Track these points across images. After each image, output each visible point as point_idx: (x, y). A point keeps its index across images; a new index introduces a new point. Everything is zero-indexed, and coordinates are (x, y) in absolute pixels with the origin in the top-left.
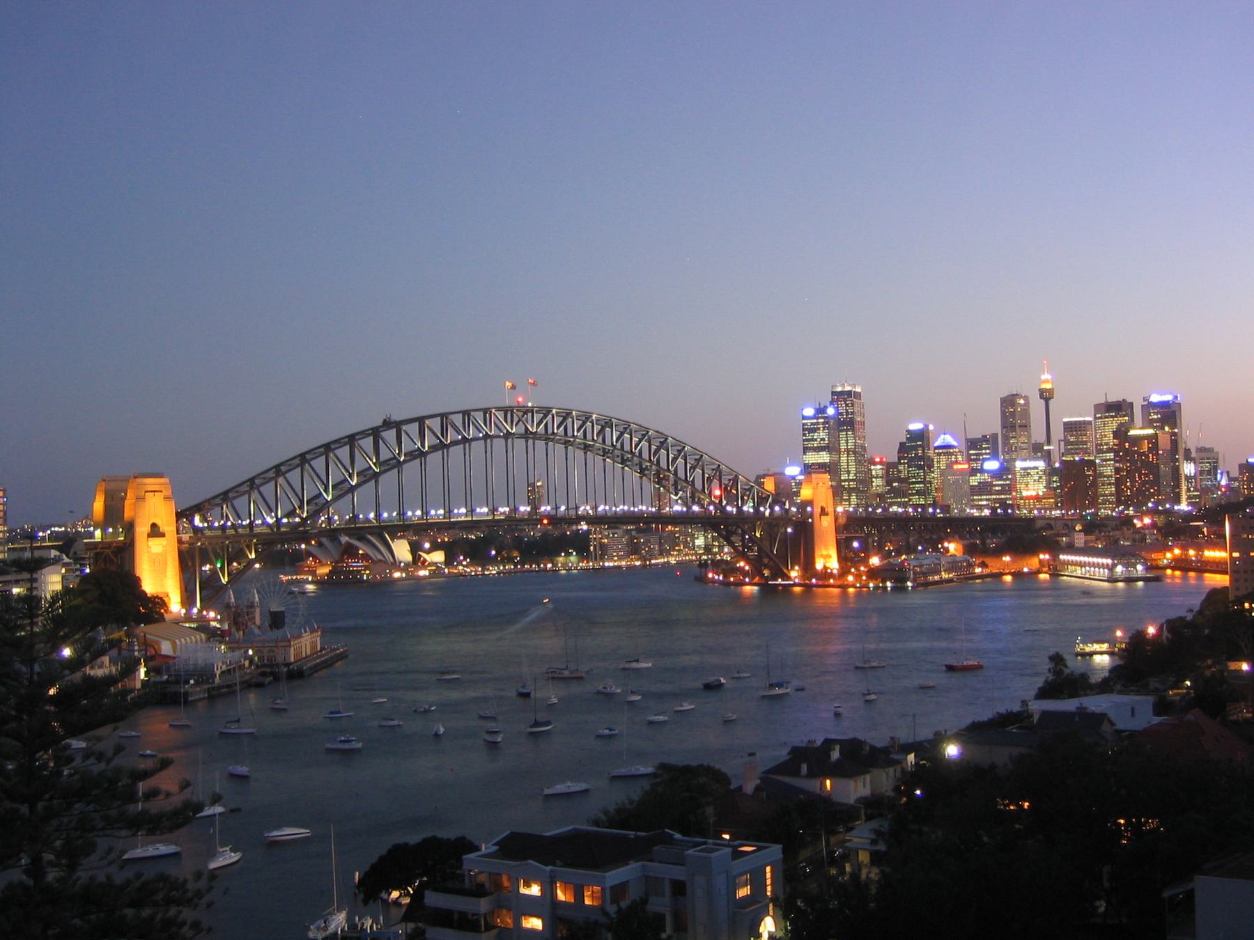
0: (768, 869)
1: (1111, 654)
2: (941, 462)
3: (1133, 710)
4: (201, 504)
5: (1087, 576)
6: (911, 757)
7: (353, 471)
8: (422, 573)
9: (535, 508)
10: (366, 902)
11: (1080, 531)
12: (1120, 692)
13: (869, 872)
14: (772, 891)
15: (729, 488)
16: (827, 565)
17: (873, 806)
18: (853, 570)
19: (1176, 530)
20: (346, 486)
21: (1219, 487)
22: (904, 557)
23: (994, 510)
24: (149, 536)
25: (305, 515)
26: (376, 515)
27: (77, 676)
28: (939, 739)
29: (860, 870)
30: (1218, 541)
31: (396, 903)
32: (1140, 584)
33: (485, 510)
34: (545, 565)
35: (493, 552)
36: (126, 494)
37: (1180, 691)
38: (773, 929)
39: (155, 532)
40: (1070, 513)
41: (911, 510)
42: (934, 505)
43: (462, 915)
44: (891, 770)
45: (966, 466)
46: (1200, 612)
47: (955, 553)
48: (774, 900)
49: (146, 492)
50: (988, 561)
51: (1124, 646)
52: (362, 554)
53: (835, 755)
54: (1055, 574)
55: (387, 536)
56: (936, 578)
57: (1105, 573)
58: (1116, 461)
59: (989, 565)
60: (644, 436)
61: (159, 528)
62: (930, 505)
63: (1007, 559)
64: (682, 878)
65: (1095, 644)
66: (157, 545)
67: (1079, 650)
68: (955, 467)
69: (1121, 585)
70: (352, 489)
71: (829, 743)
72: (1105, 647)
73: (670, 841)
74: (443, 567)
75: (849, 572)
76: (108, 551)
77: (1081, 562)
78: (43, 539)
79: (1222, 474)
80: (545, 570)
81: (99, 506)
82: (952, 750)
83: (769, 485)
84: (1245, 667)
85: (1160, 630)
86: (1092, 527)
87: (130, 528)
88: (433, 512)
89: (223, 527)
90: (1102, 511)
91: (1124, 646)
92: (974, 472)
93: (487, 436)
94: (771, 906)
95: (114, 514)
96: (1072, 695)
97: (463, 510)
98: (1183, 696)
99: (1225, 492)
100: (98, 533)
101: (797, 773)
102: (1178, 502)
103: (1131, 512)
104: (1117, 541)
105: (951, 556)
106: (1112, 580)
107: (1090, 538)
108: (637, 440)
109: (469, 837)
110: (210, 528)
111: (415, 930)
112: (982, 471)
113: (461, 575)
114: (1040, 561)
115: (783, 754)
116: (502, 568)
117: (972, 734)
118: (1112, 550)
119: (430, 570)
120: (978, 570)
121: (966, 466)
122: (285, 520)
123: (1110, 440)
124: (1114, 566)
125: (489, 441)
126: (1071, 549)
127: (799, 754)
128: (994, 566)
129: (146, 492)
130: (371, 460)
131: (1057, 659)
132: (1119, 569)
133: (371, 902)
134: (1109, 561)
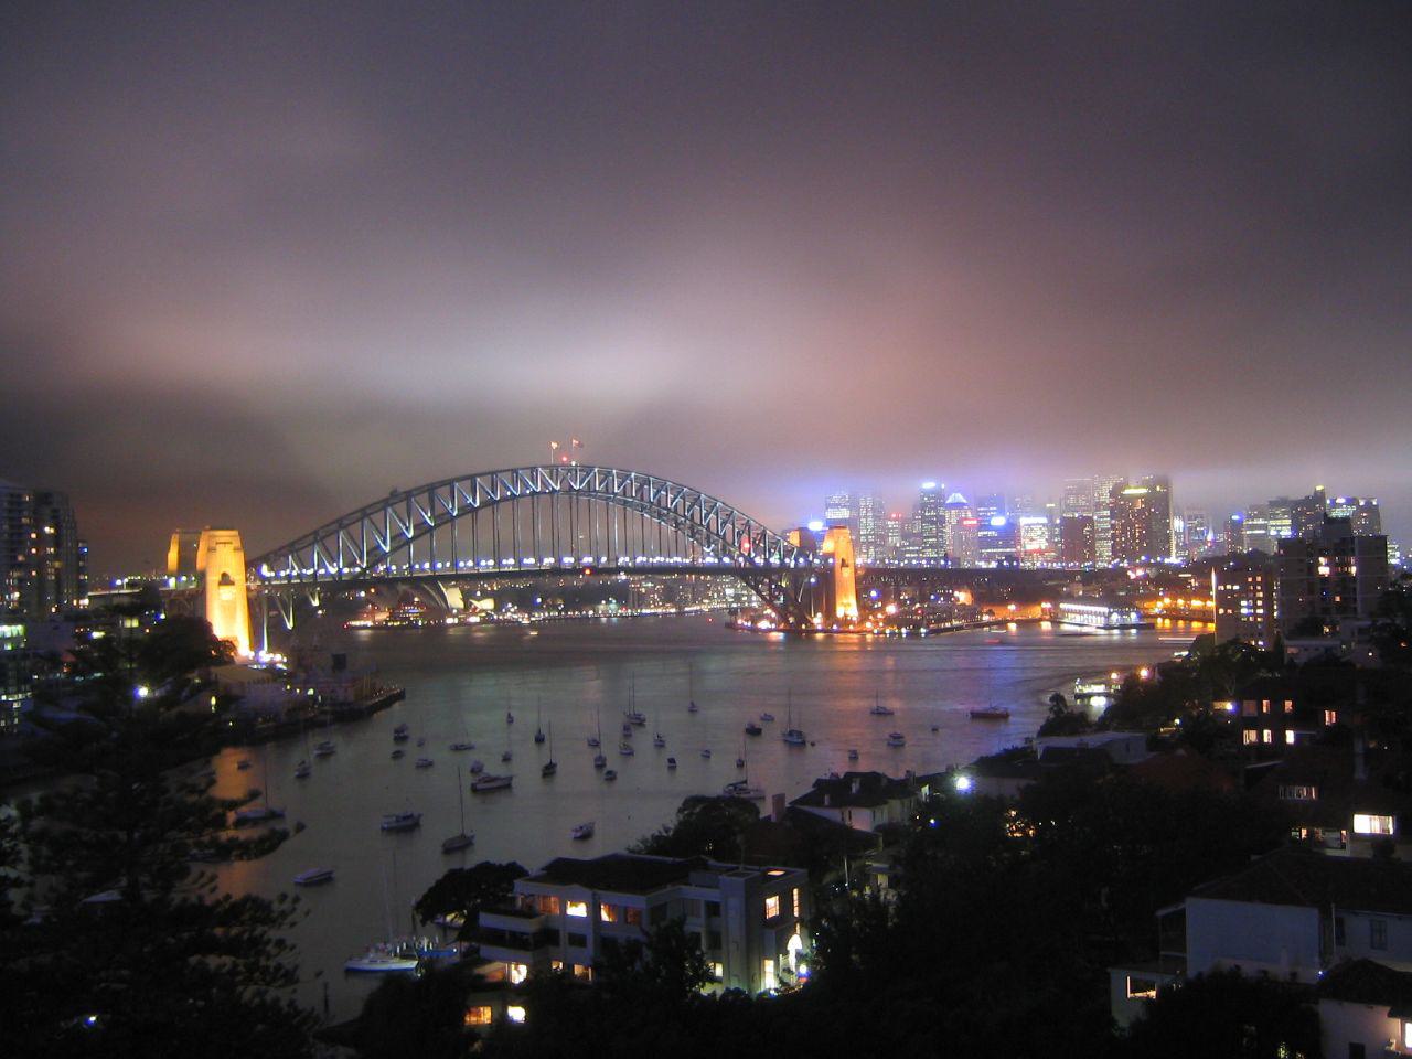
0: (796, 891)
1: (1107, 695)
2: (951, 517)
3: (1128, 746)
4: (268, 555)
6: (925, 789)
8: (474, 619)
9: (578, 560)
10: (424, 922)
11: (1080, 582)
12: (1116, 729)
13: (886, 894)
14: (800, 911)
16: (848, 613)
17: (890, 833)
18: (871, 617)
19: (1169, 581)
20: (403, 539)
21: (1205, 543)
22: (918, 605)
23: (1000, 562)
24: (220, 584)
25: (365, 565)
27: (174, 711)
28: (951, 771)
29: (879, 891)
30: (1203, 592)
32: (1134, 631)
33: (552, 560)
35: (539, 600)
38: (800, 947)
39: (225, 580)
41: (924, 562)
42: (946, 557)
43: (513, 934)
44: (906, 802)
45: (975, 522)
48: (801, 920)
50: (994, 609)
53: (855, 788)
54: (1056, 622)
56: (948, 625)
57: (1101, 621)
60: (679, 493)
62: (941, 558)
63: (1012, 607)
64: (717, 900)
68: (965, 522)
69: (1116, 632)
70: (409, 541)
71: (850, 776)
72: (1101, 688)
73: (706, 867)
78: (121, 587)
80: (587, 617)
81: (173, 556)
82: (963, 783)
83: (795, 539)
84: (1229, 706)
86: (1091, 578)
87: (202, 577)
88: (462, 564)
89: (289, 577)
92: (982, 527)
93: (534, 493)
94: (798, 926)
95: (187, 564)
96: (1073, 732)
97: (512, 561)
98: (1173, 733)
100: (172, 582)
101: (820, 804)
102: (1169, 556)
103: (1125, 564)
104: (1113, 591)
106: (1108, 627)
107: (1088, 588)
109: (519, 863)
110: (277, 577)
111: (468, 949)
112: (989, 527)
113: (509, 621)
114: (1043, 610)
115: (808, 789)
116: (547, 614)
117: (985, 767)
118: (1111, 600)
120: (986, 618)
121: (975, 522)
122: (346, 570)
123: (1106, 498)
124: (1110, 614)
125: (535, 497)
126: (1071, 598)
127: (822, 786)
128: (1000, 614)
130: (426, 514)
131: (1058, 699)
132: (1115, 617)
133: (429, 922)
134: (1105, 610)
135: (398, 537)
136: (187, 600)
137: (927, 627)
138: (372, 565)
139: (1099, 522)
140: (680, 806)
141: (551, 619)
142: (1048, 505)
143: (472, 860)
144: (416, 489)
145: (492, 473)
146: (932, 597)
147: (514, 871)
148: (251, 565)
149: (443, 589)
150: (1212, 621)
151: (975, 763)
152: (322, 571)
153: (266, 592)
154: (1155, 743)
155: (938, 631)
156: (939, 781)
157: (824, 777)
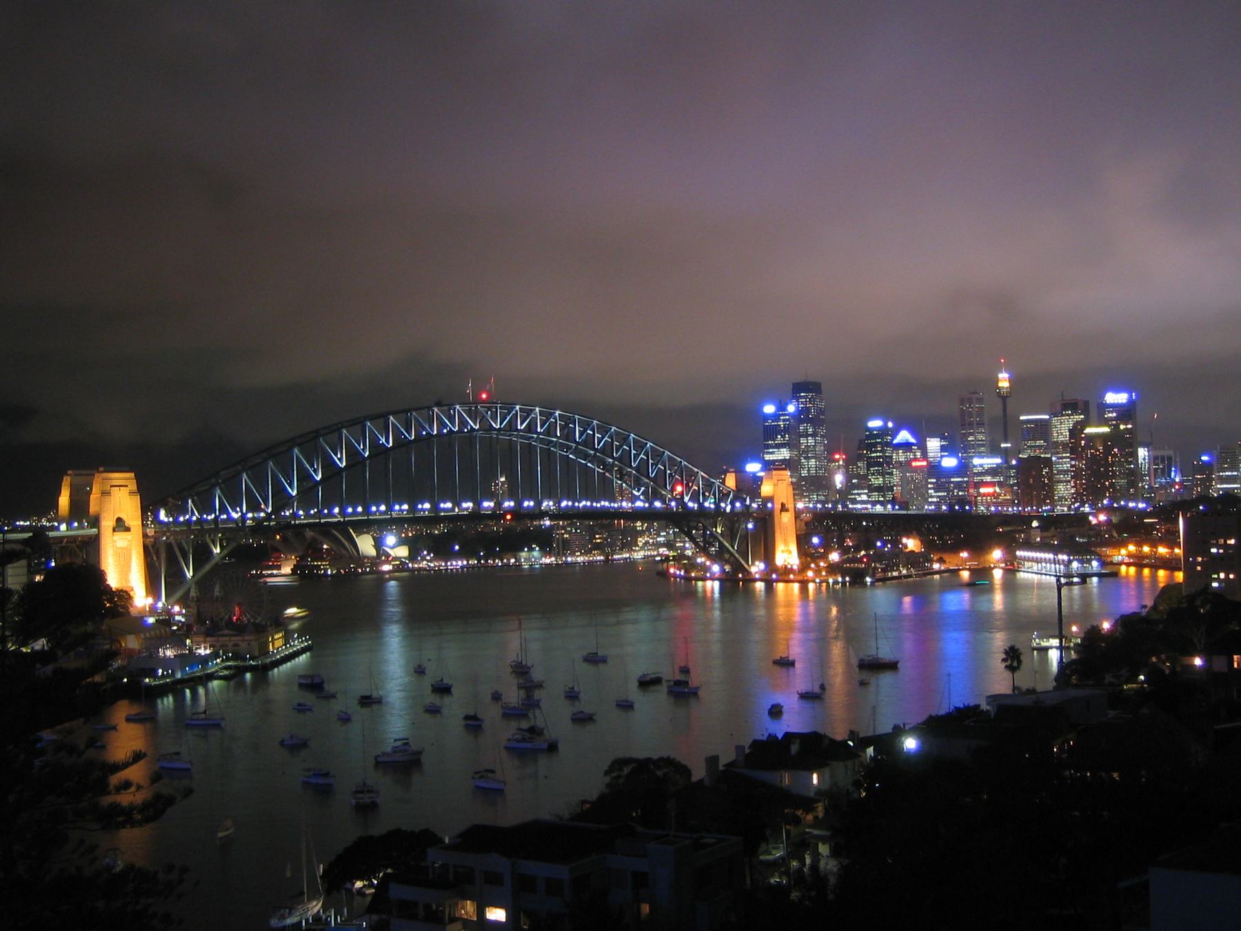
5: (1043, 572)
6: (870, 751)
7: (318, 466)
8: (386, 568)
9: (499, 504)
12: (1076, 686)
15: (690, 484)
18: (813, 565)
21: (1173, 483)
22: (863, 553)
25: (270, 510)
26: (340, 510)
28: (898, 731)
29: (819, 861)
31: (360, 892)
32: (1095, 579)
34: (509, 560)
36: (91, 489)
37: (1134, 685)
39: (120, 525)
40: (1026, 510)
42: (893, 502)
44: (850, 763)
46: (1154, 607)
47: (914, 549)
49: (111, 486)
50: (946, 557)
51: (1079, 641)
52: (327, 549)
53: (795, 748)
55: (351, 530)
56: (895, 574)
58: (1072, 459)
59: (948, 560)
61: (125, 522)
62: (889, 502)
63: (964, 555)
65: (1051, 640)
66: (121, 540)
67: (1035, 645)
68: (914, 464)
74: (407, 561)
75: (810, 568)
76: (74, 545)
77: (1037, 558)
79: (1175, 471)
80: (508, 565)
81: (64, 500)
82: (910, 744)
85: (1115, 625)
86: (1049, 523)
87: (95, 522)
89: (188, 522)
90: (1058, 507)
91: (1079, 641)
95: (80, 509)
98: (1137, 691)
99: (1179, 489)
103: (1087, 509)
104: (1073, 537)
105: (909, 552)
107: (1045, 534)
108: (600, 436)
113: (425, 569)
116: (465, 563)
119: (394, 565)
120: (936, 566)
122: (250, 515)
124: (1070, 562)
126: (1029, 545)
128: (951, 563)
129: (111, 486)
130: (336, 455)
132: (1075, 565)
134: (1065, 557)
135: (305, 477)
136: (78, 547)
137: (873, 576)
138: (277, 510)
139: (1059, 463)
140: (607, 768)
141: (468, 566)
142: (1003, 445)
143: (380, 828)
144: (325, 428)
145: (406, 411)
146: (879, 544)
147: (427, 839)
148: (148, 508)
149: (354, 535)
150: (1179, 569)
151: (924, 723)
152: (224, 516)
153: (164, 538)
154: (1117, 700)
155: (884, 580)
156: (886, 744)
157: (761, 738)
